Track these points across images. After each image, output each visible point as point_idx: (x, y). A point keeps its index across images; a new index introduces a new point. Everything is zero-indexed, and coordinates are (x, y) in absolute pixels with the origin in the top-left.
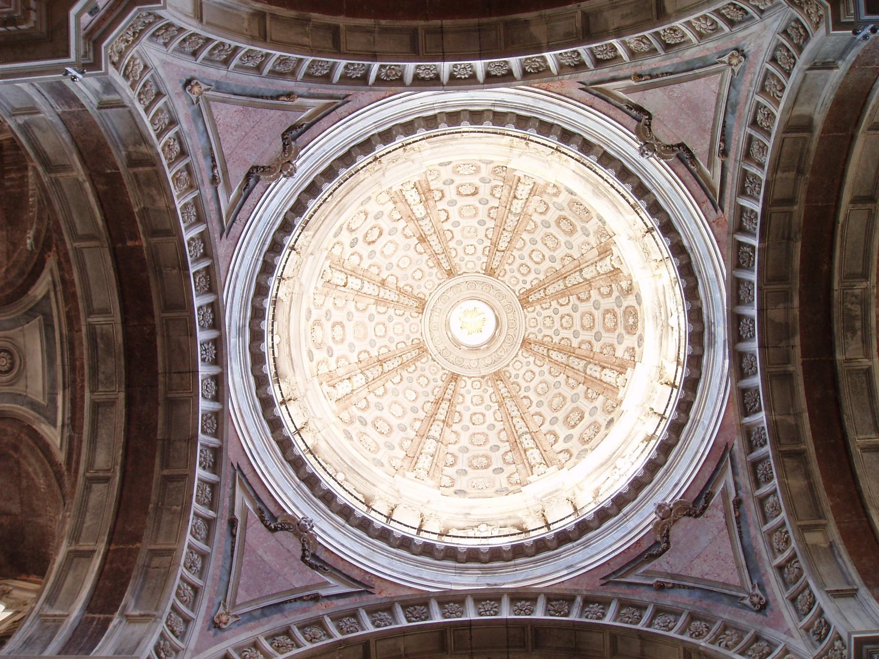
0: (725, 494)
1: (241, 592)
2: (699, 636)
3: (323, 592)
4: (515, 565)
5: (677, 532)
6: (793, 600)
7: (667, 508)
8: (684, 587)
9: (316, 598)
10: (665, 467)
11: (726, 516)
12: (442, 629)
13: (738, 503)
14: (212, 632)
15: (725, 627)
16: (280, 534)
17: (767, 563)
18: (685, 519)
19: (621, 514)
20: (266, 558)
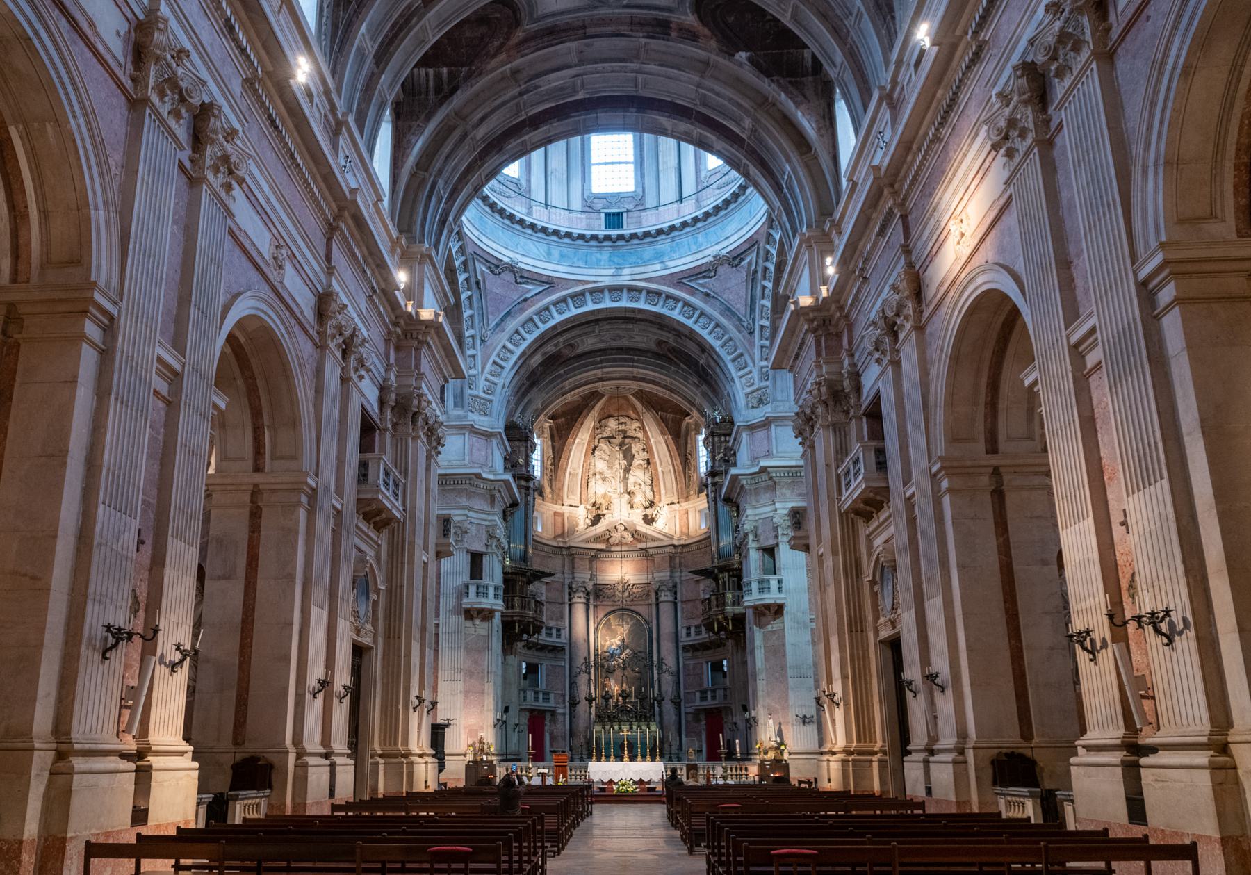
0: (750, 263)
2: (718, 338)
3: (528, 296)
5: (721, 270)
9: (525, 300)
12: (592, 312)
15: (731, 339)
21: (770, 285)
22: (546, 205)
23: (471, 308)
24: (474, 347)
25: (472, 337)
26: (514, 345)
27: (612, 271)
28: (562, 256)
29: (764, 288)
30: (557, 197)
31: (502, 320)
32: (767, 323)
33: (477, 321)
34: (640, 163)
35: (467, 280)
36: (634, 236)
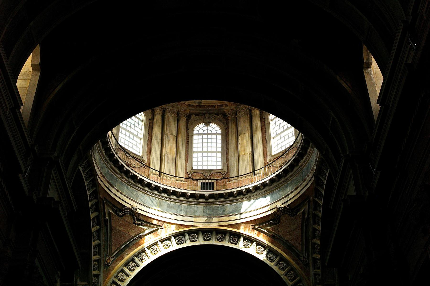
0: (304, 213)
1: (113, 247)
3: (143, 234)
4: (219, 202)
6: (315, 274)
7: (281, 209)
8: (282, 241)
10: (285, 178)
11: (303, 222)
13: (308, 219)
14: (105, 269)
16: (124, 217)
17: (310, 255)
18: (287, 215)
19: (264, 190)
20: (120, 229)
21: (319, 228)
22: (160, 172)
23: (99, 239)
24: (98, 269)
25: (98, 261)
26: (130, 270)
27: (205, 219)
28: (168, 206)
29: (315, 230)
30: (168, 168)
31: (122, 251)
32: (318, 256)
33: (102, 250)
34: (226, 152)
35: (97, 217)
36: (221, 196)
